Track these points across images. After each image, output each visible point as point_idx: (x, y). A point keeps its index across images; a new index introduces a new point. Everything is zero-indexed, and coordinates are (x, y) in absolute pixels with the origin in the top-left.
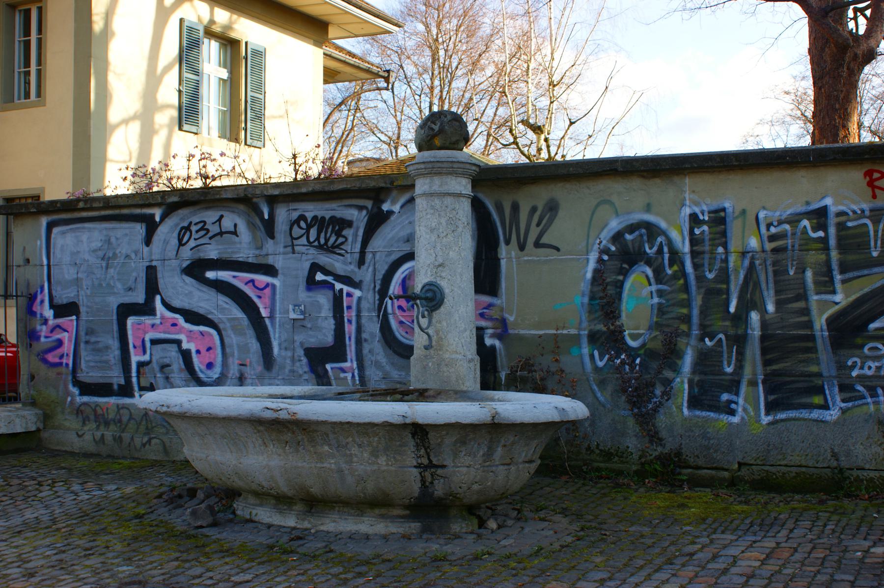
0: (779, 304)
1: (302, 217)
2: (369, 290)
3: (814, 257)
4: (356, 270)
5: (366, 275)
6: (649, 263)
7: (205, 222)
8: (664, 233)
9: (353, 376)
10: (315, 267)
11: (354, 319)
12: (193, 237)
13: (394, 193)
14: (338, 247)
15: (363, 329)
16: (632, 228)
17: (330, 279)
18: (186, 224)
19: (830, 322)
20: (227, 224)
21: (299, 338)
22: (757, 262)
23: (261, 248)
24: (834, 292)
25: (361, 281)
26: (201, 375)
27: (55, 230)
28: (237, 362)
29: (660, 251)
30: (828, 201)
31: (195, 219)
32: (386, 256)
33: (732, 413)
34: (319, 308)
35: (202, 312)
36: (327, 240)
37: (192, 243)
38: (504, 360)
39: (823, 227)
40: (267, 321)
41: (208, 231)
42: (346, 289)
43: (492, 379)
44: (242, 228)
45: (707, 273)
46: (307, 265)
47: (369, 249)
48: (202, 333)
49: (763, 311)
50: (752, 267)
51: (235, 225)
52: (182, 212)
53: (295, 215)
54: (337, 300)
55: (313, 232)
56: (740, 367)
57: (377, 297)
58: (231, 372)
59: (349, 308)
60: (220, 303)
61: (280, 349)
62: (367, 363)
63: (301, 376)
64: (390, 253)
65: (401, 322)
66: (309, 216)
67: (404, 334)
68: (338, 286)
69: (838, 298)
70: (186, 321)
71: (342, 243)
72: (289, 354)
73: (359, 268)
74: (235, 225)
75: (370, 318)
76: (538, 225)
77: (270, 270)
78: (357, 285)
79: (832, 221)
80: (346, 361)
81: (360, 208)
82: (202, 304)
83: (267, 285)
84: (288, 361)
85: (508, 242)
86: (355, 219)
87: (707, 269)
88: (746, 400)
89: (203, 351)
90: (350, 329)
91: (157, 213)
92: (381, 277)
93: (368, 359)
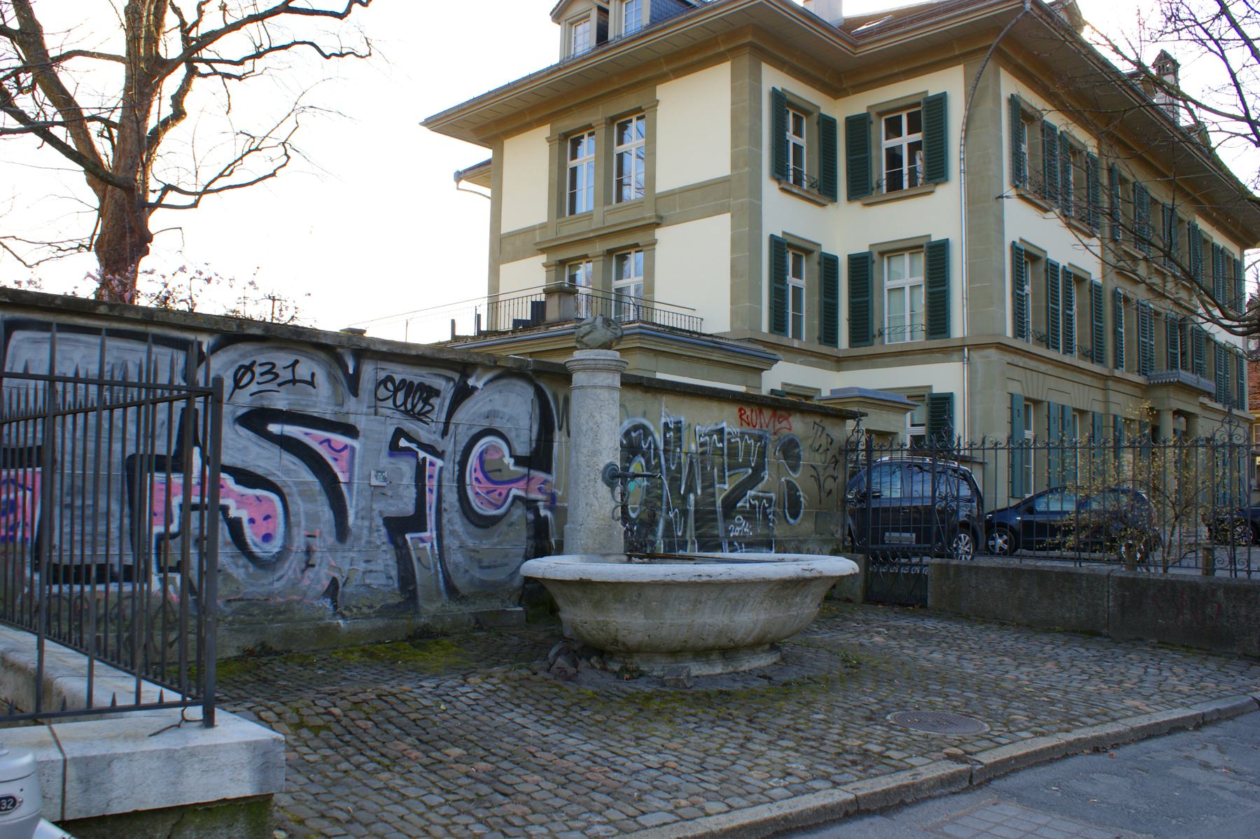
0: (703, 489)
1: (390, 379)
3: (718, 460)
5: (447, 445)
6: (643, 456)
7: (274, 365)
8: (652, 435)
9: (432, 546)
10: (399, 433)
11: (435, 489)
12: (256, 380)
13: (479, 370)
14: (424, 414)
16: (636, 428)
17: (413, 446)
18: (247, 362)
19: (723, 502)
20: (303, 371)
21: (377, 506)
23: (342, 405)
25: (443, 452)
26: (255, 549)
27: (18, 336)
28: (303, 533)
29: (649, 448)
30: (724, 425)
31: (261, 359)
34: (401, 475)
35: (260, 472)
36: (414, 406)
37: (254, 387)
39: (721, 440)
40: (343, 487)
41: (277, 376)
42: (429, 458)
44: (321, 378)
46: (391, 430)
47: (453, 420)
48: (258, 498)
49: (696, 494)
50: (691, 463)
51: (313, 375)
52: (243, 347)
53: (382, 375)
54: (420, 468)
55: (400, 397)
56: (685, 532)
57: (457, 468)
58: (296, 544)
59: (431, 477)
60: (285, 462)
61: (356, 518)
62: (446, 532)
63: (378, 547)
64: (471, 427)
65: (477, 493)
66: (398, 378)
68: (422, 454)
69: (726, 487)
70: (237, 482)
71: (429, 412)
72: (366, 523)
74: (313, 375)
77: (351, 431)
78: (440, 455)
79: (726, 437)
80: (425, 530)
81: (449, 379)
82: (261, 463)
83: (346, 447)
84: (365, 532)
85: (560, 429)
89: (259, 519)
90: (431, 499)
91: (206, 341)
93: (447, 528)
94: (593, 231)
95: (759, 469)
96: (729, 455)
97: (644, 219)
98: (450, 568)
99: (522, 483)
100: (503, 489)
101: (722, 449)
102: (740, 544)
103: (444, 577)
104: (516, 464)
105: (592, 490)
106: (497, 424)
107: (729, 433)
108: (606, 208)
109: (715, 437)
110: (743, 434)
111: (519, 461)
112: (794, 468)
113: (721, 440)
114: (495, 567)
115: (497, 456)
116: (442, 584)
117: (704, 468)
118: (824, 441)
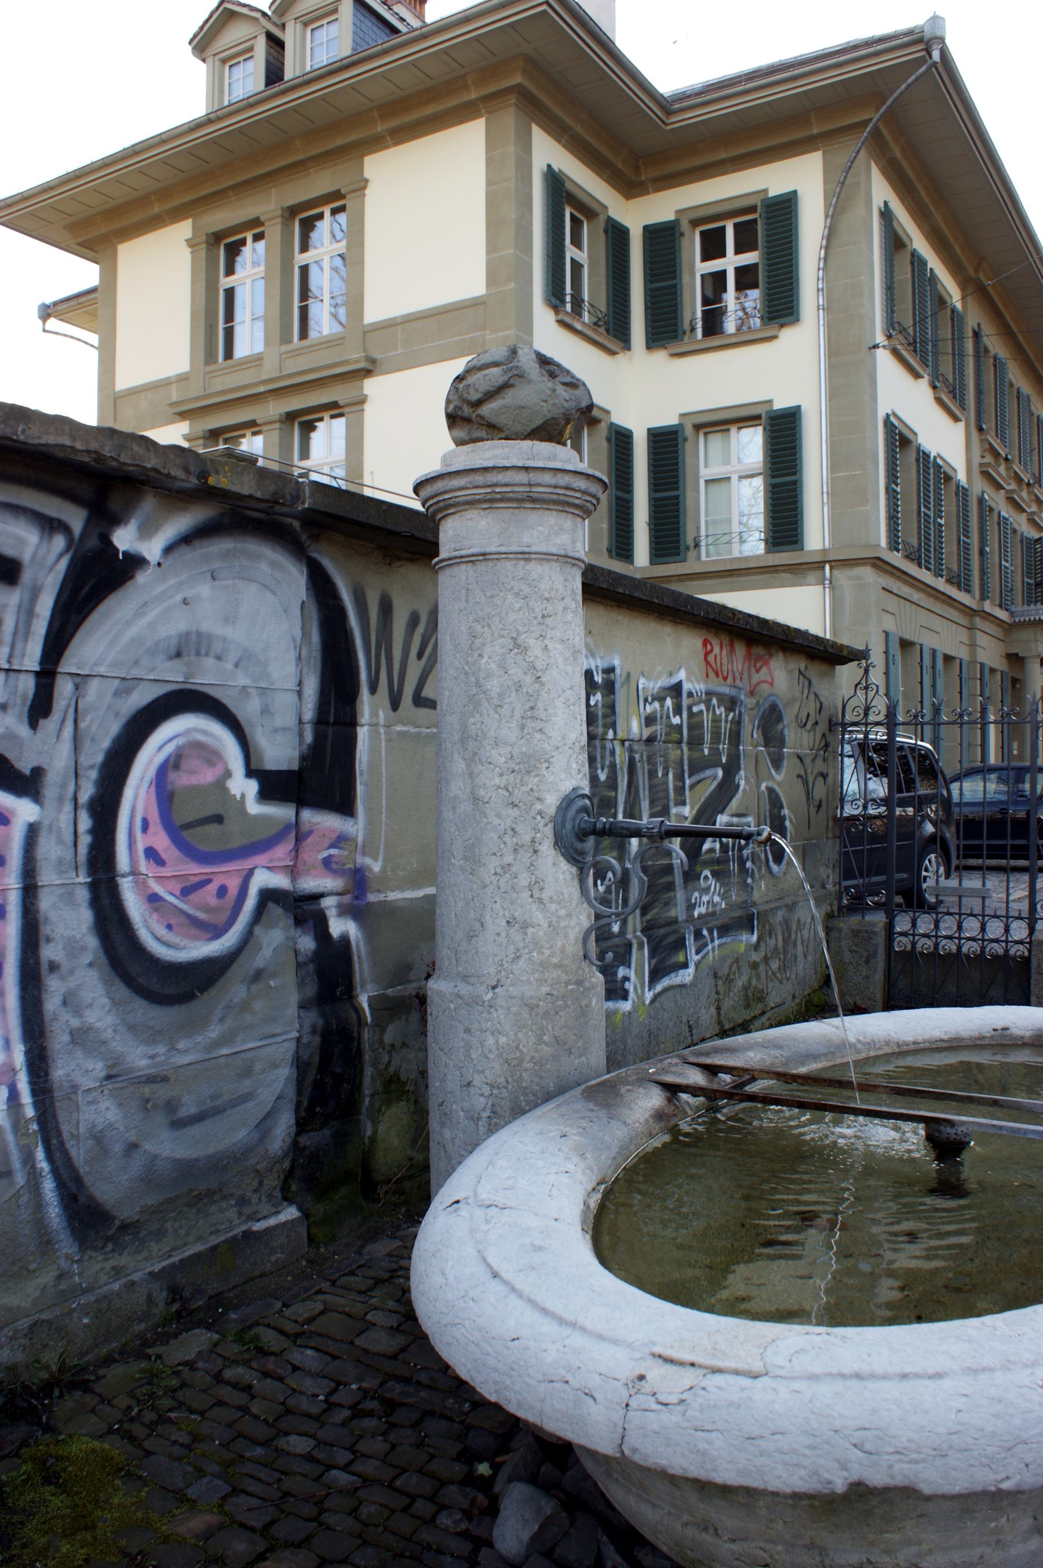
2: (61, 800)
3: (674, 754)
4: (23, 730)
5: (49, 749)
13: (149, 504)
15: (45, 930)
22: (637, 756)
24: (684, 803)
25: (38, 772)
30: (682, 675)
32: (117, 693)
33: (625, 997)
38: (365, 966)
43: (354, 1017)
45: (599, 771)
47: (69, 664)
57: (85, 822)
62: (58, 1039)
64: (127, 685)
65: (153, 899)
67: (163, 932)
73: (33, 724)
75: (68, 893)
76: (420, 656)
79: (685, 702)
81: (50, 525)
85: (373, 689)
86: (26, 557)
87: (599, 766)
88: (636, 974)
92: (100, 758)
94: (258, 384)
95: (731, 769)
96: (689, 743)
97: (346, 362)
98: (79, 1154)
99: (282, 852)
100: (228, 874)
101: (679, 727)
102: (711, 932)
103: (61, 1185)
104: (265, 795)
105: (524, 880)
106: (206, 677)
107: (690, 694)
108: (285, 348)
109: (669, 702)
110: (709, 694)
111: (274, 786)
112: (777, 762)
113: (678, 710)
114: (217, 1111)
115: (208, 776)
116: (54, 1211)
117: (652, 774)
118: (811, 707)
